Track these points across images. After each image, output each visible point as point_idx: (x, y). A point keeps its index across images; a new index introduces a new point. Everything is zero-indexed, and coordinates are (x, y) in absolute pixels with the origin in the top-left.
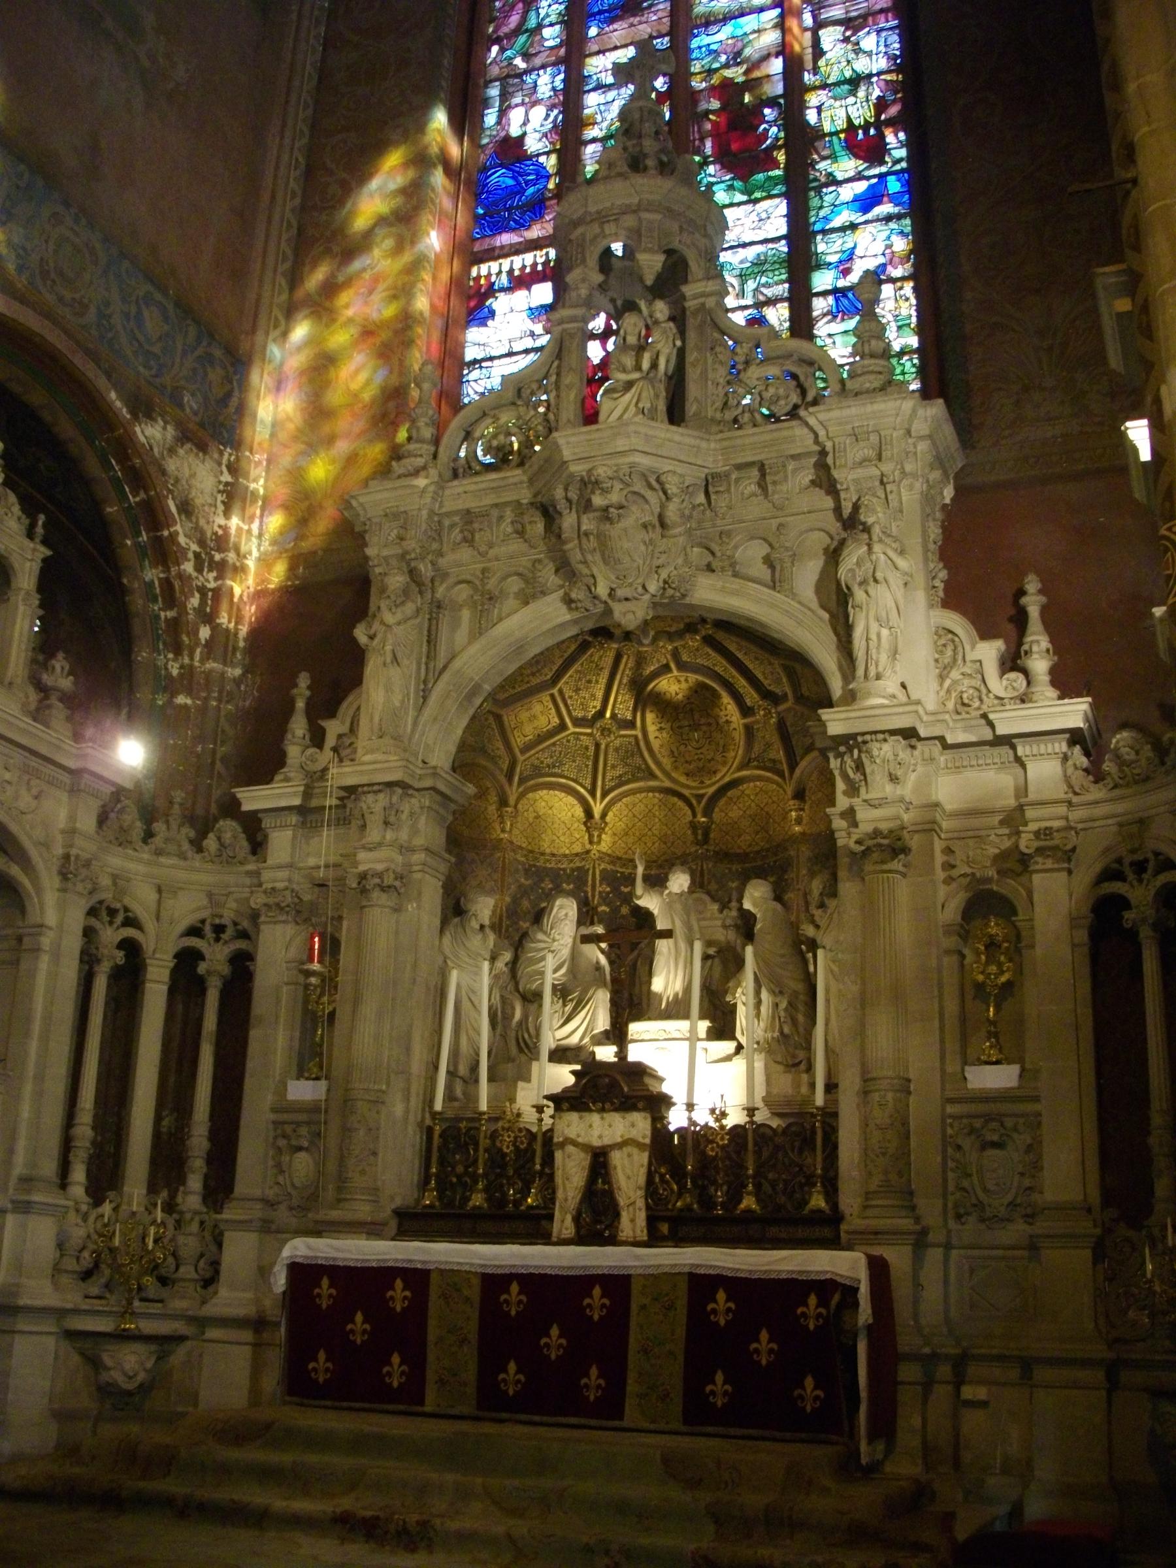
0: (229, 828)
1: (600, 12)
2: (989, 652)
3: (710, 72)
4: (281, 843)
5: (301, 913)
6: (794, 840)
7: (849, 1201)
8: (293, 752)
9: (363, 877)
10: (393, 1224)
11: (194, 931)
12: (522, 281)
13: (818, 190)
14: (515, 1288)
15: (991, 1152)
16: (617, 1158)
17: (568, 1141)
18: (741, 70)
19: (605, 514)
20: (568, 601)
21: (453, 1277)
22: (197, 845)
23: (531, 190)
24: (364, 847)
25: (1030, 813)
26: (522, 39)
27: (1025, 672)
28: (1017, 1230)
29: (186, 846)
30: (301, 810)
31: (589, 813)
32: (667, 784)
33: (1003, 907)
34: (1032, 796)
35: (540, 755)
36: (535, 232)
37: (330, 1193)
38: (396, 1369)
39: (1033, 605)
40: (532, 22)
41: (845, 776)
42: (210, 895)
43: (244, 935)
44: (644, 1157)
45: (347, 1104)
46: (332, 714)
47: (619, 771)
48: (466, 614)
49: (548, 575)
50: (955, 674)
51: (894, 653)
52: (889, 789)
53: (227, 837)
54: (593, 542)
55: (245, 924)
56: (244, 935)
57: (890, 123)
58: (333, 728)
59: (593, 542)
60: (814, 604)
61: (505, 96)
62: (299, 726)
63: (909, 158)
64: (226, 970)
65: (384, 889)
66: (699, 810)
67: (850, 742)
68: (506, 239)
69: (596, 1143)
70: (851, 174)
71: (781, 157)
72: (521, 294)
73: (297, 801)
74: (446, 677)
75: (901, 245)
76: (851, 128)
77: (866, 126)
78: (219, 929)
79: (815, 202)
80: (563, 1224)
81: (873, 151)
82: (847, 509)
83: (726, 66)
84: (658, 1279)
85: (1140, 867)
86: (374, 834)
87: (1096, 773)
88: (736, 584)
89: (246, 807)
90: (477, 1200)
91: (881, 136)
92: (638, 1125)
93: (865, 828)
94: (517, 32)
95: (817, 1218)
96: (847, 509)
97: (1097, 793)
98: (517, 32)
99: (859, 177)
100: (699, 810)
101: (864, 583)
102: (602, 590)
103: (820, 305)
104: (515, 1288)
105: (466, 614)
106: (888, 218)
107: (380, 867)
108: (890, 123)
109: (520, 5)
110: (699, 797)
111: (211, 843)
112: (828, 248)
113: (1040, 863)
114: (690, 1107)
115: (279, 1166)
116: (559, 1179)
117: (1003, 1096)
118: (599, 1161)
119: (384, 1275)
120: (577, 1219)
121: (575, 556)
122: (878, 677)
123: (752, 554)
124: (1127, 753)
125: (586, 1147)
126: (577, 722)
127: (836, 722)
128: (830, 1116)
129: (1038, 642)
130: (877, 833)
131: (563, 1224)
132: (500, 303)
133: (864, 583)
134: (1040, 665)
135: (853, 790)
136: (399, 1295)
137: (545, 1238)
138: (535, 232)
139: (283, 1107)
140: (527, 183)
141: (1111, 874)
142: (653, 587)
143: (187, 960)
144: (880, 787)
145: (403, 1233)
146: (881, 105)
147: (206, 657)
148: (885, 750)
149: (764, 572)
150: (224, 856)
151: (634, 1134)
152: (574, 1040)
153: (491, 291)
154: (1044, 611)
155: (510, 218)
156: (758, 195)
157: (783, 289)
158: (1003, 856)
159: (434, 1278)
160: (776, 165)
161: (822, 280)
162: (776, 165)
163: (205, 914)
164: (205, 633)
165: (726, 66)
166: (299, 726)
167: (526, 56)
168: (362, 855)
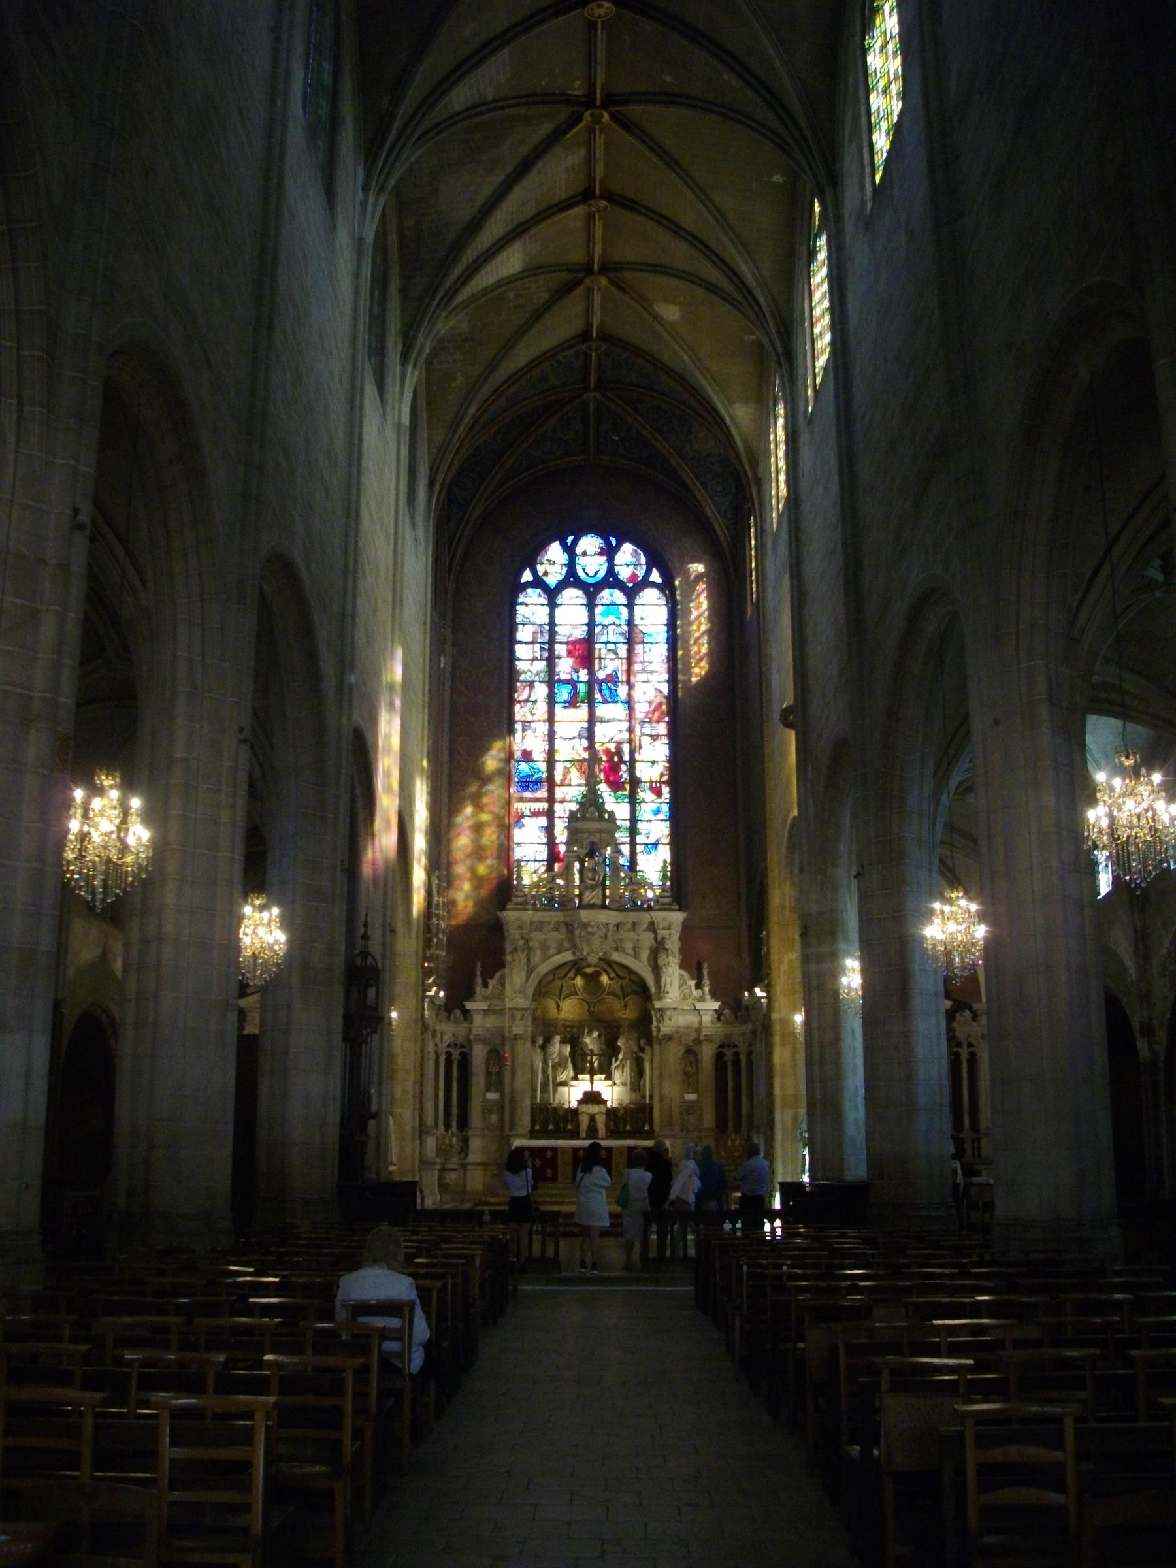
0: (458, 1012)
1: (560, 702)
2: (693, 983)
3: (603, 744)
4: (478, 1020)
5: (485, 1042)
6: (622, 1019)
7: (656, 1128)
8: (479, 989)
9: (515, 1035)
10: (528, 1135)
11: (449, 1046)
12: (535, 814)
13: (640, 803)
14: (581, 1151)
15: (691, 1116)
16: (597, 1117)
17: (583, 1112)
18: (615, 745)
19: (590, 933)
20: (574, 954)
21: (564, 1150)
22: (449, 1018)
23: (536, 776)
24: (516, 1026)
25: (703, 1030)
26: (529, 704)
27: (702, 990)
28: (695, 1134)
29: (446, 1019)
30: (485, 1010)
31: (558, 1006)
32: (582, 997)
33: (695, 1054)
34: (703, 1025)
35: (547, 989)
36: (538, 795)
37: (507, 1127)
38: (549, 1172)
39: (705, 971)
40: (532, 699)
41: (656, 1017)
42: (454, 1035)
43: (462, 1046)
44: (604, 1117)
45: (513, 1100)
46: (492, 978)
47: (567, 992)
48: (538, 952)
49: (566, 945)
50: (683, 988)
51: (671, 984)
52: (669, 1022)
53: (458, 1015)
54: (584, 939)
55: (465, 1044)
56: (462, 1046)
57: (664, 783)
58: (491, 983)
59: (584, 939)
60: (646, 963)
61: (524, 730)
62: (479, 980)
63: (670, 798)
64: (459, 1057)
65: (521, 1039)
66: (592, 1006)
67: (660, 1010)
68: (527, 795)
69: (591, 1113)
70: (651, 800)
71: (627, 787)
72: (534, 819)
73: (486, 1008)
74: (535, 972)
75: (667, 831)
76: (651, 782)
77: (656, 782)
78: (456, 1045)
79: (638, 808)
80: (583, 1134)
81: (658, 792)
82: (659, 940)
83: (608, 742)
84: (619, 1148)
85: (729, 1046)
86: (518, 1022)
87: (719, 1019)
88: (624, 956)
89: (467, 1008)
90: (551, 1127)
91: (660, 787)
92: (602, 1108)
93: (662, 1033)
94: (527, 701)
95: (647, 1132)
96: (659, 940)
97: (719, 1025)
98: (527, 701)
99: (653, 802)
100: (592, 1006)
101: (665, 965)
102: (585, 953)
103: (639, 848)
104: (581, 1151)
105: (538, 952)
106: (662, 820)
107: (521, 1033)
108: (664, 783)
109: (528, 688)
110: (592, 1002)
111: (452, 1017)
112: (641, 826)
113: (705, 1043)
114: (612, 1102)
115: (485, 1118)
116: (580, 1122)
117: (694, 1102)
118: (592, 1118)
119: (545, 1149)
120: (587, 1133)
121: (578, 941)
122: (668, 993)
123: (629, 946)
124: (728, 1016)
125: (587, 1114)
126: (559, 979)
127: (657, 1005)
128: (651, 1107)
129: (706, 982)
130: (665, 1035)
131: (583, 1134)
132: (525, 821)
133: (665, 965)
134: (706, 989)
135: (659, 1021)
136: (549, 1154)
137: (578, 1138)
138: (538, 795)
139: (485, 1101)
140: (535, 772)
141: (721, 1046)
142: (601, 954)
143: (448, 1054)
144: (667, 1022)
145: (531, 1138)
146: (662, 775)
147: (437, 949)
148: (669, 1013)
149: (631, 952)
150: (456, 1022)
151: (601, 1110)
152: (564, 1079)
153: (522, 816)
154: (708, 973)
155: (528, 786)
156: (619, 800)
157: (628, 839)
158: (695, 1040)
159: (559, 1151)
160: (625, 790)
161: (640, 839)
162: (625, 790)
163: (452, 1040)
164: (435, 940)
165: (608, 742)
166: (479, 980)
167: (533, 715)
168: (514, 1028)
